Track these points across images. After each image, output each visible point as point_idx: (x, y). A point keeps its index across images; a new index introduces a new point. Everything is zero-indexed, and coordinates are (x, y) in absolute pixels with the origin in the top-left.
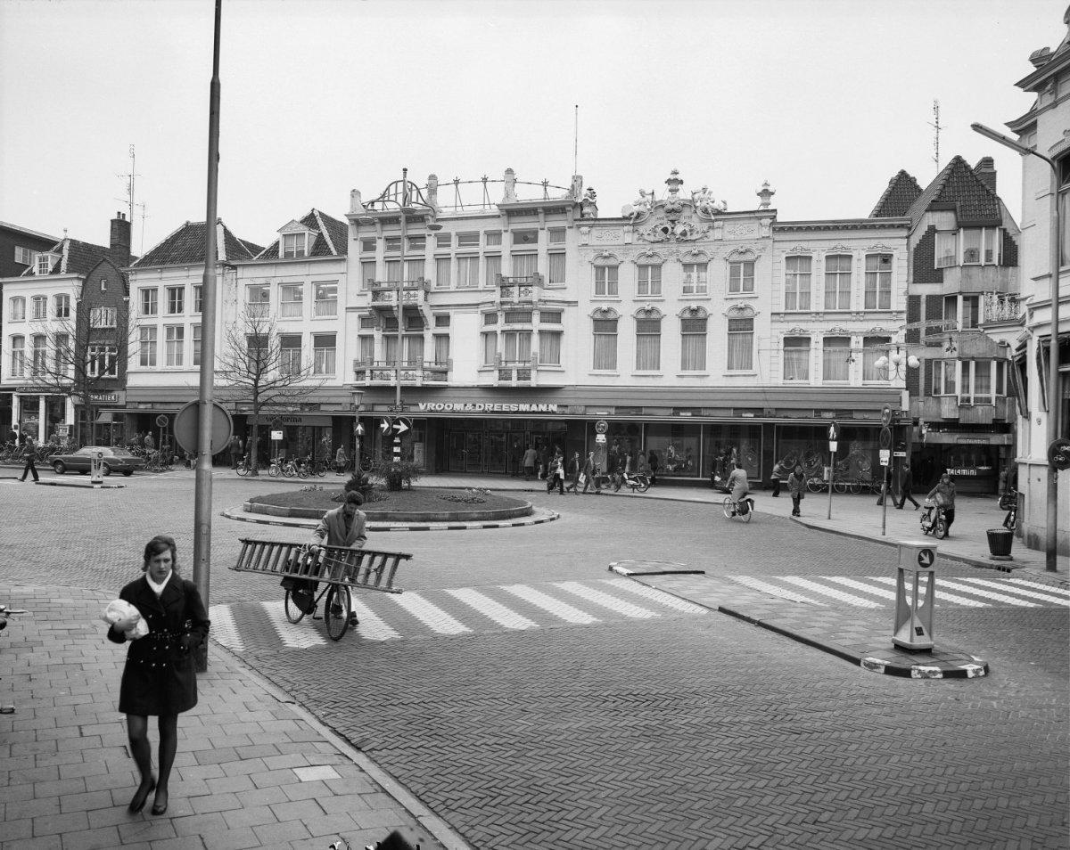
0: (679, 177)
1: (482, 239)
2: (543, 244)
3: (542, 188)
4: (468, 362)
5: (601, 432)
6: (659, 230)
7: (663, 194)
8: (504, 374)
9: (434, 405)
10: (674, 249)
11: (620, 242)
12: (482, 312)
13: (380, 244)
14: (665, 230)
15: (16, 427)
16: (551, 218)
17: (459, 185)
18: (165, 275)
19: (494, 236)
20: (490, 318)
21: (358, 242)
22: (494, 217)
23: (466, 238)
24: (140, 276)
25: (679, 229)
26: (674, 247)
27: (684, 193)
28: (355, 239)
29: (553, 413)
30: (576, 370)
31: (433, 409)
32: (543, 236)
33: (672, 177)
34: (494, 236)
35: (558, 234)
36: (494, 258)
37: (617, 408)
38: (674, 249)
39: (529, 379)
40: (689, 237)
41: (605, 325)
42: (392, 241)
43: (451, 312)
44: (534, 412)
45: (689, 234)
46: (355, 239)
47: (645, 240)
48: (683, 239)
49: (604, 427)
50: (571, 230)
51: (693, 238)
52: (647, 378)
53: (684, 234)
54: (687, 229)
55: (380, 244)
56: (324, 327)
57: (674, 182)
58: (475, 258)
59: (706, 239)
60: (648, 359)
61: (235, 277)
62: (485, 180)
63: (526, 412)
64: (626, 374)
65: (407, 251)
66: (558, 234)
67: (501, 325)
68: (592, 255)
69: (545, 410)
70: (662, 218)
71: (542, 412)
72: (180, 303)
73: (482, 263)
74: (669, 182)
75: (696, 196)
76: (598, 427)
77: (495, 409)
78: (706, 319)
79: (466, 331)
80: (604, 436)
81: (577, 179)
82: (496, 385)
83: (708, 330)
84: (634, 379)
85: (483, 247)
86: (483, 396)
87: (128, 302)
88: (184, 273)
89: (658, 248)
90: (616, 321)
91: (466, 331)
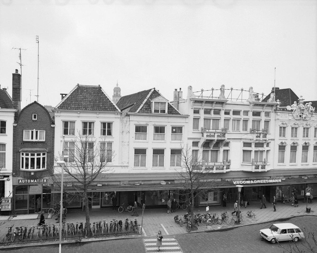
1: (242, 113)
2: (263, 117)
4: (236, 161)
5: (308, 192)
6: (299, 116)
8: (257, 167)
10: (302, 123)
11: (287, 119)
12: (243, 142)
13: (202, 112)
14: (300, 116)
15: (84, 229)
17: (233, 91)
18: (81, 115)
19: (246, 113)
20: (246, 144)
22: (247, 105)
23: (236, 113)
24: (62, 114)
25: (304, 116)
26: (302, 122)
28: (192, 108)
29: (280, 182)
30: (276, 163)
32: (263, 114)
34: (246, 113)
35: (267, 114)
36: (246, 121)
37: (284, 176)
38: (302, 123)
40: (306, 119)
41: (282, 148)
42: (207, 112)
43: (231, 141)
46: (192, 108)
47: (295, 119)
48: (305, 120)
49: (310, 190)
52: (294, 166)
53: (305, 118)
55: (202, 112)
56: (177, 146)
58: (238, 120)
59: (310, 120)
60: (293, 160)
61: (128, 120)
62: (242, 90)
64: (287, 165)
65: (212, 115)
66: (267, 114)
67: (253, 148)
68: (280, 123)
69: (277, 182)
70: (299, 112)
72: (90, 130)
73: (241, 123)
76: (307, 190)
77: (261, 182)
78: (308, 146)
79: (236, 150)
80: (309, 193)
82: (253, 171)
83: (309, 149)
84: (290, 166)
85: (242, 116)
86: (244, 174)
87: (54, 128)
88: (95, 115)
89: (298, 122)
90: (285, 146)
91: (236, 150)
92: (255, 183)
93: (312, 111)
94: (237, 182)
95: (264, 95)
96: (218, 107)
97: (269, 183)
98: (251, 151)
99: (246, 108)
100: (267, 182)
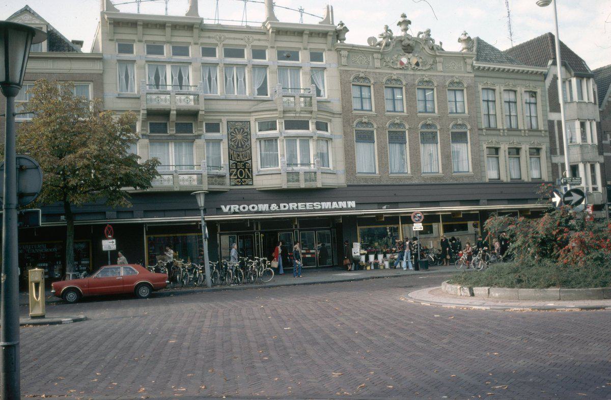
0: (408, 18)
3: (299, 14)
5: (418, 221)
7: (398, 32)
9: (237, 206)
16: (176, 33)
21: (112, 43)
27: (413, 32)
29: (352, 209)
31: (295, 208)
33: (401, 20)
35: (316, 56)
39: (315, 180)
44: (336, 209)
45: (420, 65)
50: (330, 52)
51: (424, 68)
53: (417, 64)
54: (420, 61)
57: (405, 23)
63: (328, 210)
69: (345, 206)
71: (342, 209)
74: (399, 24)
75: (421, 36)
76: (414, 217)
77: (300, 208)
80: (421, 224)
81: (330, 10)
82: (285, 186)
92: (282, 208)
93: (433, 47)
94: (232, 206)
95: (305, 11)
96: (181, 38)
97: (321, 210)
98: (276, 139)
99: (259, 42)
100: (316, 208)
